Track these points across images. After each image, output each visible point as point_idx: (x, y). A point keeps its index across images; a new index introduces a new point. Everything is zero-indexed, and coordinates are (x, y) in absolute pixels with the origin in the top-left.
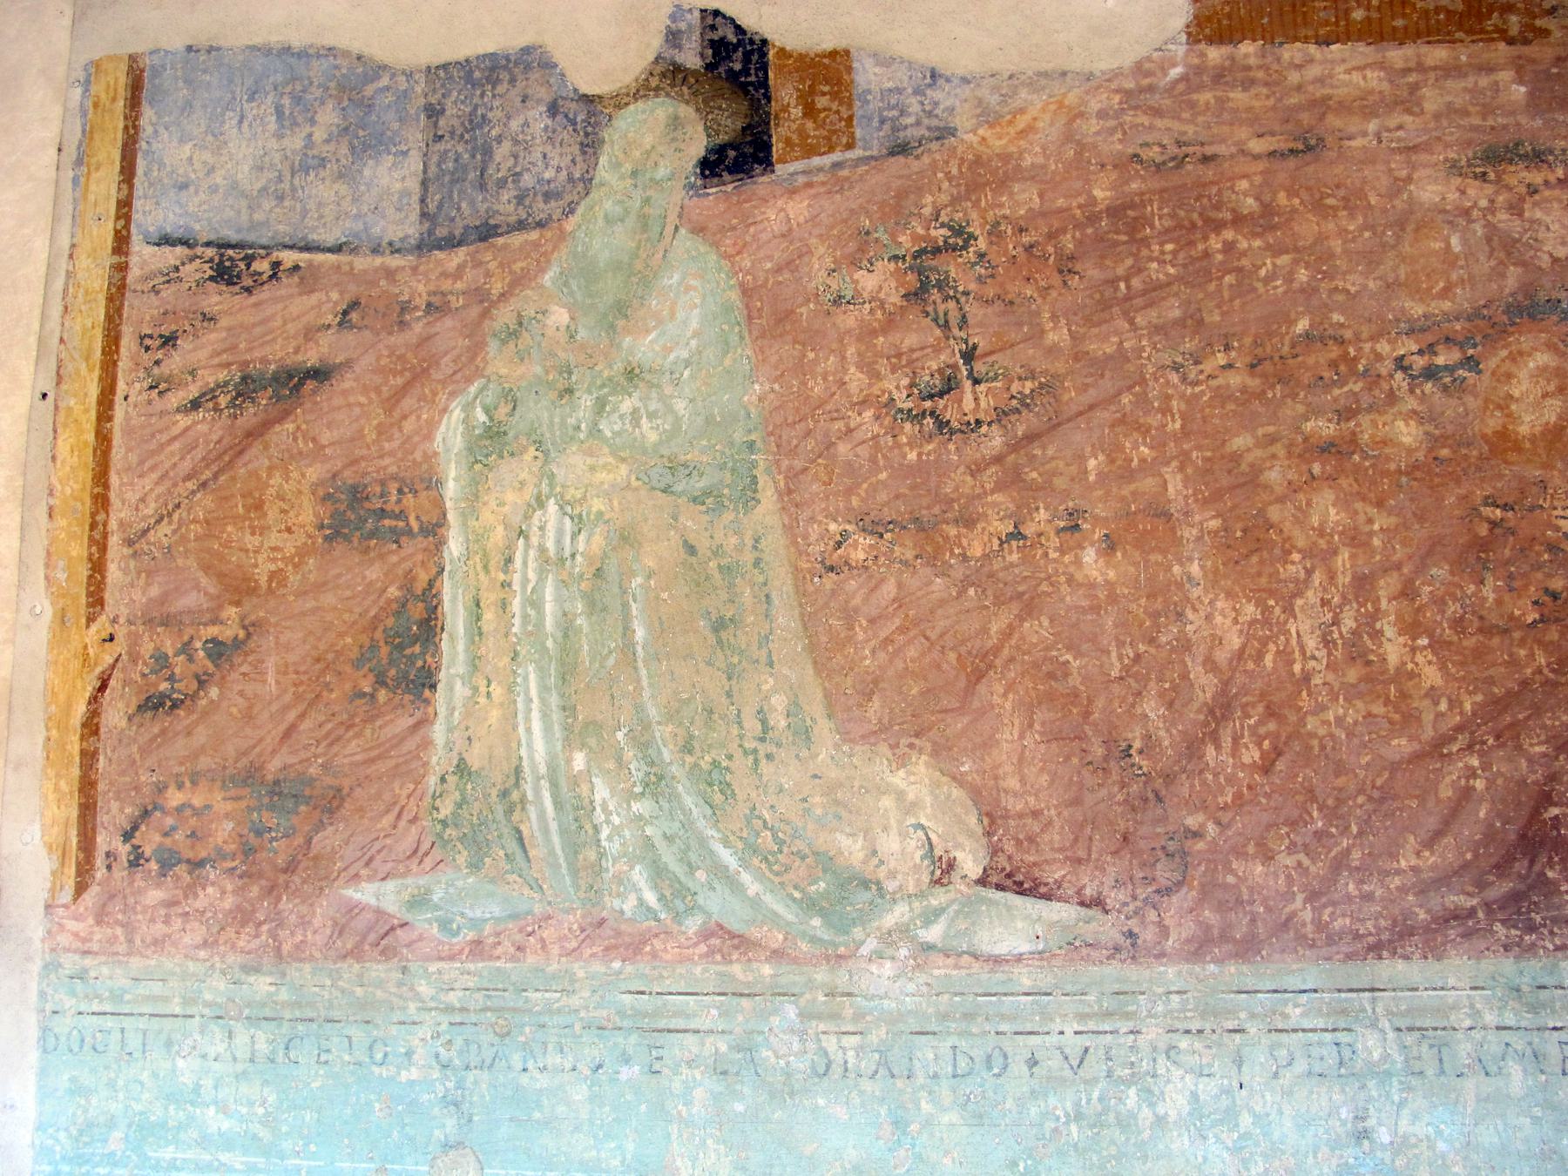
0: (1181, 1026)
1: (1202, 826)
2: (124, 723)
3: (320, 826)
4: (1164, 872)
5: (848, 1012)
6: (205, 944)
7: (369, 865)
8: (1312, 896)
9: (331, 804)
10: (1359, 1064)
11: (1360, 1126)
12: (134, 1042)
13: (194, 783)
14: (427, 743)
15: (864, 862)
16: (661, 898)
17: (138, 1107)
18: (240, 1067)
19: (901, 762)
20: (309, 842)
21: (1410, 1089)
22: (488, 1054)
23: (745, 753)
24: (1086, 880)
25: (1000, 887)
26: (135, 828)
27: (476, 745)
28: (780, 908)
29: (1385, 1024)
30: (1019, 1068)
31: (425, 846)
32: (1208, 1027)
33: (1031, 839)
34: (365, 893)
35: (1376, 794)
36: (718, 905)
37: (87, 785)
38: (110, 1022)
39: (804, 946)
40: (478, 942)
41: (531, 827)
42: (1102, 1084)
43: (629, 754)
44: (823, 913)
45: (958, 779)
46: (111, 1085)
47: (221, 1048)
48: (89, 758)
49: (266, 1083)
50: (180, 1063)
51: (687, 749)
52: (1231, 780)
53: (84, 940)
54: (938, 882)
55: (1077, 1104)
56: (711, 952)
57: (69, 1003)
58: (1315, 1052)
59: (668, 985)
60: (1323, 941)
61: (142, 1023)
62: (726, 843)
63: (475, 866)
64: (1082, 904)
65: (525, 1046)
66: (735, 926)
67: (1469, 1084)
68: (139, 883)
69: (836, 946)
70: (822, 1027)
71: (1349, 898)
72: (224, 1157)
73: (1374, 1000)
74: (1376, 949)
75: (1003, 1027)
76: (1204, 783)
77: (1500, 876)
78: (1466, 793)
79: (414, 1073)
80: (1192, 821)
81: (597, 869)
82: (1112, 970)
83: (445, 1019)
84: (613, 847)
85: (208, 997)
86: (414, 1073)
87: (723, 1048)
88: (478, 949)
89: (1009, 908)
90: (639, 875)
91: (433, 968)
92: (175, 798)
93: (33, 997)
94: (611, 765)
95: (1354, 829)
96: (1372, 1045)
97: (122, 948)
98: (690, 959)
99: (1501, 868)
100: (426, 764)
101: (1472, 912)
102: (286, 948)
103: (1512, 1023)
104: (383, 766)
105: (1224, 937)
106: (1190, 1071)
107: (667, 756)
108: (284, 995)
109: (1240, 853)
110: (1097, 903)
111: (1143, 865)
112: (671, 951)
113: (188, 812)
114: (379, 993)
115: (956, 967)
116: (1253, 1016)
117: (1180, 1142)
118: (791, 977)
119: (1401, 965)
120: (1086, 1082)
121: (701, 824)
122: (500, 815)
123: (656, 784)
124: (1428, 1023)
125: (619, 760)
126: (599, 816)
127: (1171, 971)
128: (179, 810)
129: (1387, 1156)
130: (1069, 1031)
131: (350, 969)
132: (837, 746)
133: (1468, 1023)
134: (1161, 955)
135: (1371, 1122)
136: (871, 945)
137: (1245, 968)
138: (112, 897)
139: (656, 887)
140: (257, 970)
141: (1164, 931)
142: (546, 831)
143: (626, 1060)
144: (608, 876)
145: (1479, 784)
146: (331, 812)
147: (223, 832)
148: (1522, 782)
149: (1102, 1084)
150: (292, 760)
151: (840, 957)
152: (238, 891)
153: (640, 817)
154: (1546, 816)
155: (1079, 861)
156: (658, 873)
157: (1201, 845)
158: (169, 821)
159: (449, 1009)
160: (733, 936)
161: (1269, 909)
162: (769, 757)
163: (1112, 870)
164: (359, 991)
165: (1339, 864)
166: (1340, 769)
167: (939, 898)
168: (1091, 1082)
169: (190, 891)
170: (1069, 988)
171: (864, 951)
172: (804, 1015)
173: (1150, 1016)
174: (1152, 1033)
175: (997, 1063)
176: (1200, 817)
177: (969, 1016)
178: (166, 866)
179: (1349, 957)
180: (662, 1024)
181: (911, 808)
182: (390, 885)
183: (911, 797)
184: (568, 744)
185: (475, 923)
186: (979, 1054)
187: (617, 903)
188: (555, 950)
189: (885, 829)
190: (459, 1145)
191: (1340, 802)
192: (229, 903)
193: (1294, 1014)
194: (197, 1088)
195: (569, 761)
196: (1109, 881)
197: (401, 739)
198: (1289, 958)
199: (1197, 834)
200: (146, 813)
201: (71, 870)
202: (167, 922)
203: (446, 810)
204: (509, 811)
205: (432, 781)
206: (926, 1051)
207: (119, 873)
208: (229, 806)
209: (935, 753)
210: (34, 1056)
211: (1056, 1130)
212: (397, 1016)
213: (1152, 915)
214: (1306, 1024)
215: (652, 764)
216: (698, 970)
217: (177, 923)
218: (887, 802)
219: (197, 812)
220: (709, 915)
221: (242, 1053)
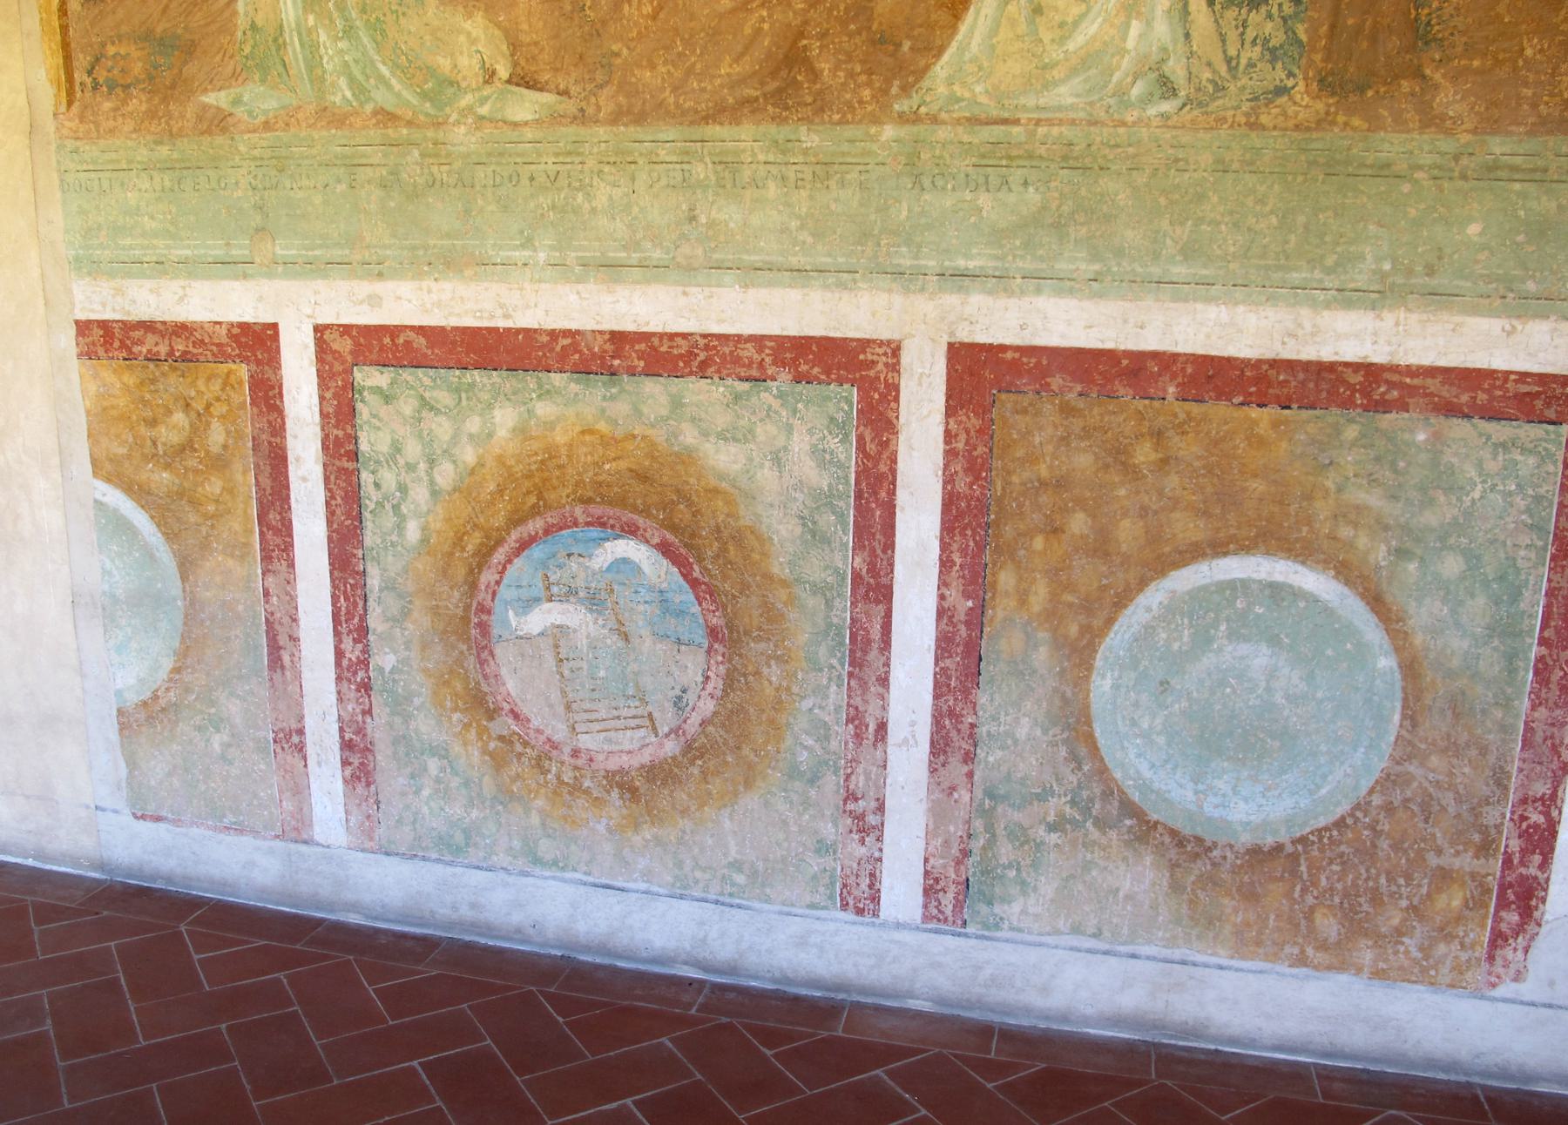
0: (605, 159)
1: (621, 50)
2: (79, 8)
3: (185, 62)
4: (600, 76)
5: (443, 153)
6: (135, 130)
7: (212, 83)
8: (675, 89)
9: (189, 50)
10: (693, 180)
11: (692, 214)
12: (106, 185)
13: (120, 41)
14: (235, 13)
15: (451, 72)
16: (354, 95)
17: (112, 219)
18: (157, 194)
19: (469, 16)
20: (181, 71)
21: (717, 194)
22: (274, 181)
23: (392, 12)
24: (560, 80)
25: (518, 85)
26: (93, 68)
27: (259, 12)
28: (410, 98)
29: (707, 160)
30: (525, 181)
31: (239, 70)
32: (619, 160)
33: (533, 58)
34: (210, 99)
35: (711, 32)
36: (381, 97)
37: (66, 46)
38: (93, 175)
39: (422, 118)
40: (267, 122)
41: (289, 57)
42: (566, 190)
43: (335, 15)
44: (431, 100)
45: (498, 25)
46: (97, 207)
47: (147, 185)
48: (64, 29)
49: (170, 202)
50: (129, 194)
51: (363, 11)
52: (636, 24)
53: (75, 132)
54: (486, 82)
55: (553, 201)
56: (378, 123)
57: (72, 166)
58: (671, 174)
59: (358, 141)
60: (681, 116)
61: (108, 174)
62: (384, 63)
63: (263, 81)
64: (558, 93)
65: (292, 176)
66: (389, 108)
67: (748, 193)
68: (99, 99)
69: (437, 117)
70: (431, 161)
71: (693, 90)
72: (155, 242)
73: (703, 147)
74: (707, 119)
75: (518, 160)
76: (622, 26)
77: (773, 79)
78: (758, 32)
79: (240, 193)
80: (615, 48)
81: (322, 79)
82: (572, 129)
83: (253, 164)
84: (329, 67)
85: (139, 158)
86: (240, 193)
87: (384, 173)
88: (267, 126)
89: (522, 96)
90: (343, 82)
91: (246, 137)
92: (111, 50)
93: (54, 164)
94: (327, 22)
95: (698, 51)
96: (700, 171)
97: (94, 135)
98: (368, 127)
99: (774, 74)
100: (235, 25)
101: (756, 99)
102: (174, 130)
103: (772, 160)
104: (213, 27)
105: (629, 112)
106: (609, 184)
107: (354, 15)
108: (175, 155)
109: (640, 66)
110: (565, 93)
111: (589, 71)
112: (358, 122)
113: (119, 58)
114: (221, 152)
115: (496, 128)
116: (641, 154)
117: (603, 221)
118: (417, 135)
119: (718, 128)
120: (558, 189)
121: (372, 52)
122: (274, 52)
123: (349, 32)
124: (730, 159)
125: (332, 21)
126: (322, 51)
127: (601, 130)
128: (114, 56)
129: (704, 230)
130: (550, 162)
131: (206, 139)
132: (437, 8)
133: (750, 160)
134: (597, 121)
135: (697, 212)
136: (454, 117)
137: (639, 129)
138: (86, 107)
139: (351, 89)
140: (161, 143)
141: (599, 108)
142: (297, 60)
143: (339, 181)
144: (328, 83)
145: (766, 26)
146: (191, 54)
147: (138, 68)
148: (789, 25)
149: (566, 190)
150: (167, 25)
151: (439, 124)
152: (149, 100)
153: (342, 50)
154: (800, 45)
155: (557, 70)
156: (352, 81)
157: (618, 61)
158: (110, 63)
159: (255, 159)
160: (388, 113)
161: (652, 96)
162: (404, 14)
163: (574, 75)
164: (211, 151)
165: (689, 72)
166: (692, 17)
167: (487, 91)
168: (559, 190)
169: (125, 102)
170: (551, 139)
171: (451, 120)
172: (423, 155)
173: (590, 154)
174: (591, 163)
175: (515, 179)
176: (620, 45)
177: (501, 154)
178: (111, 89)
179: (692, 123)
180: (355, 162)
181: (474, 41)
182: (223, 94)
183: (474, 34)
184: (305, 11)
185: (265, 112)
186: (505, 174)
187: (332, 98)
188: (304, 125)
189: (461, 53)
190: (263, 229)
191: (692, 36)
192: (144, 107)
193: (663, 154)
194: (138, 209)
195: (306, 20)
196: (572, 81)
197: (222, 11)
198: (661, 123)
199: (617, 55)
200: (97, 60)
201: (64, 94)
202: (115, 120)
203: (247, 50)
204: (278, 50)
205: (239, 34)
206: (480, 173)
207: (88, 94)
208: (139, 53)
209: (486, 10)
210: (59, 194)
211: (542, 215)
212: (231, 163)
213: (593, 100)
214: (668, 159)
215: (347, 20)
216: (372, 133)
217: (120, 120)
218: (462, 38)
219: (124, 58)
220: (376, 103)
221: (158, 188)
